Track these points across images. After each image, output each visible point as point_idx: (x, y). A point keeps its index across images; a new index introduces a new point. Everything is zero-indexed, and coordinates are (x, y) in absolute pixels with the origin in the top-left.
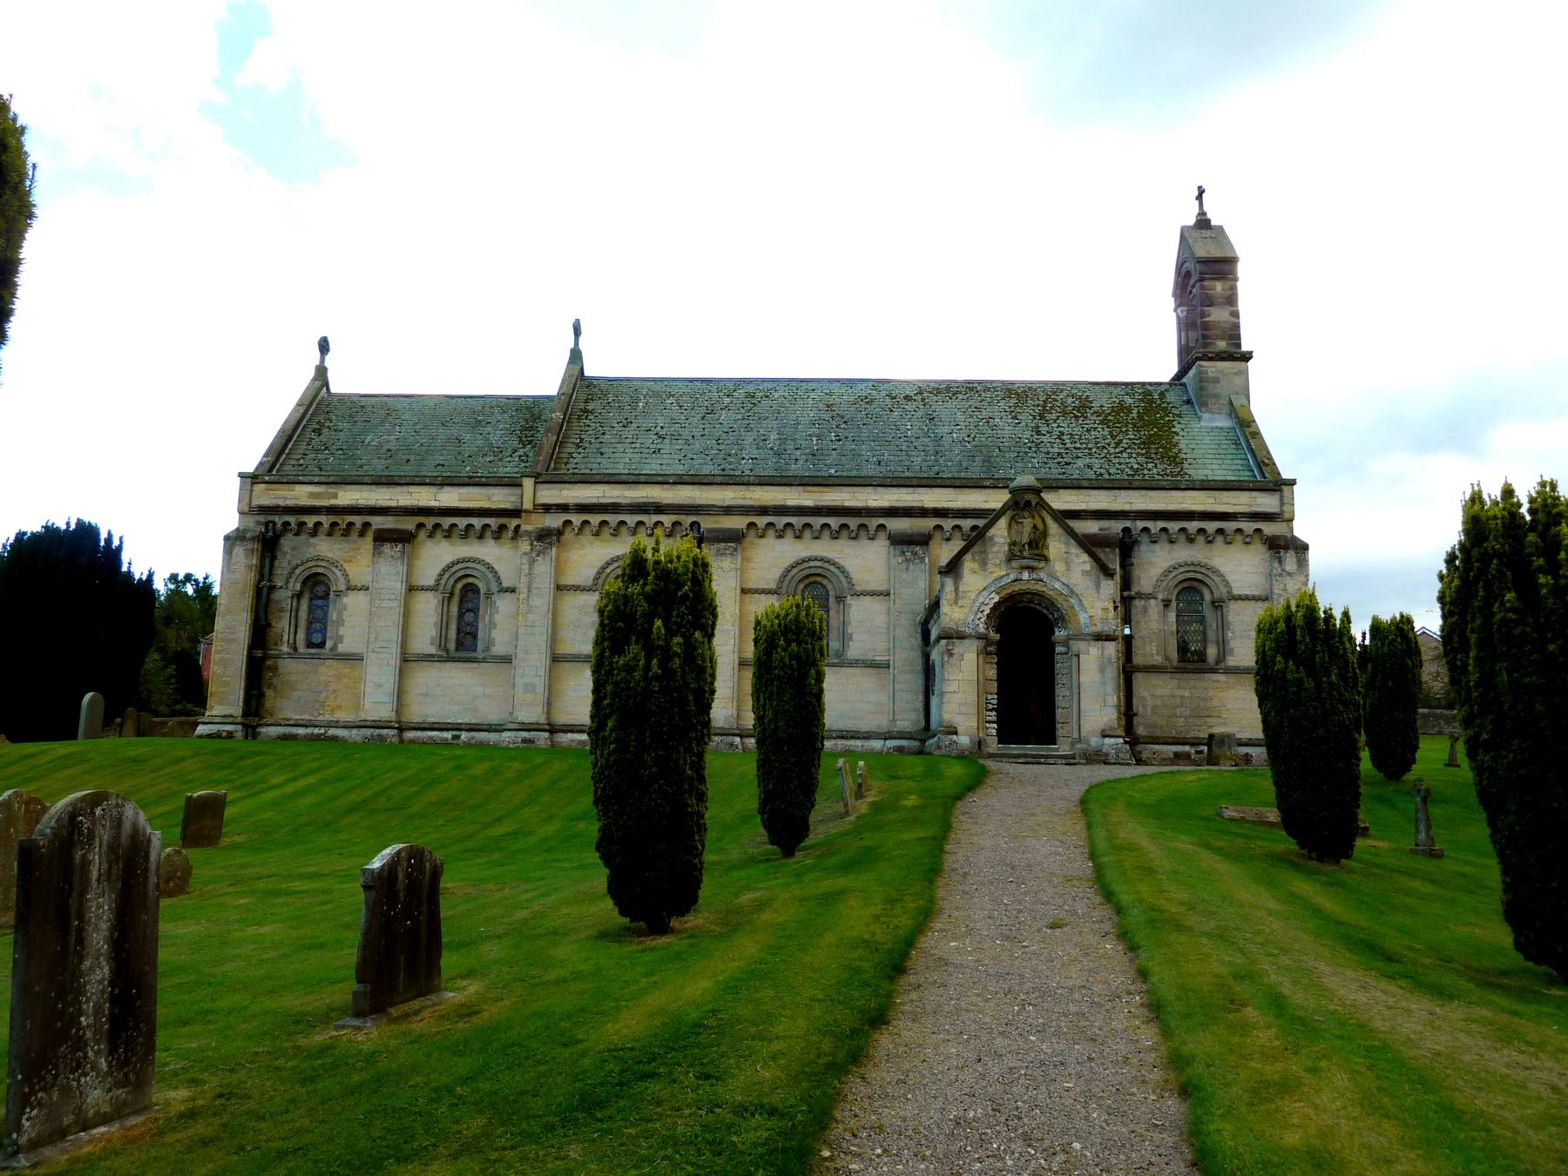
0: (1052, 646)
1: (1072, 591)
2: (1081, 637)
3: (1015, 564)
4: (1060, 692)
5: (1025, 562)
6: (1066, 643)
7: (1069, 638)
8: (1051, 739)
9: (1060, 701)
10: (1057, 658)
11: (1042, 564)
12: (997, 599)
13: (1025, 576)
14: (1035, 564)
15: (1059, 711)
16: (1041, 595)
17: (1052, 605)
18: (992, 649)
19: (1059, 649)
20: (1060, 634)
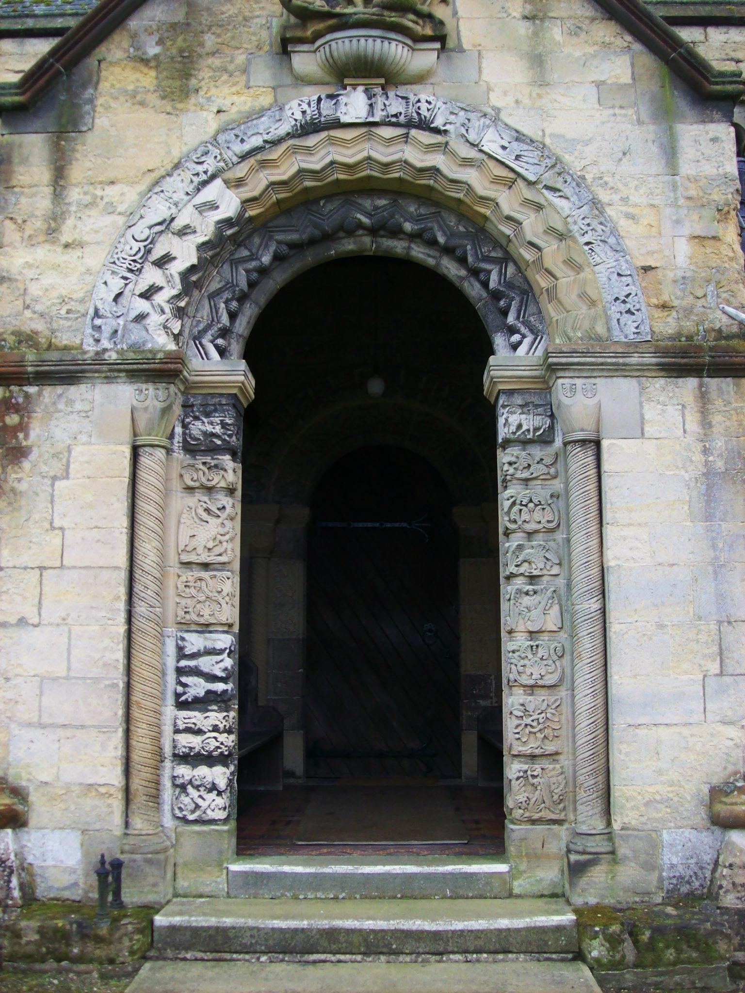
0: (485, 415)
1: (557, 165)
2: (605, 360)
3: (305, 62)
4: (523, 614)
5: (345, 44)
6: (539, 392)
7: (552, 369)
8: (477, 814)
9: (521, 659)
10: (504, 457)
11: (425, 59)
12: (229, 205)
13: (354, 105)
14: (396, 51)
15: (513, 701)
16: (420, 192)
17: (473, 228)
18: (198, 428)
19: (511, 421)
20: (510, 360)
